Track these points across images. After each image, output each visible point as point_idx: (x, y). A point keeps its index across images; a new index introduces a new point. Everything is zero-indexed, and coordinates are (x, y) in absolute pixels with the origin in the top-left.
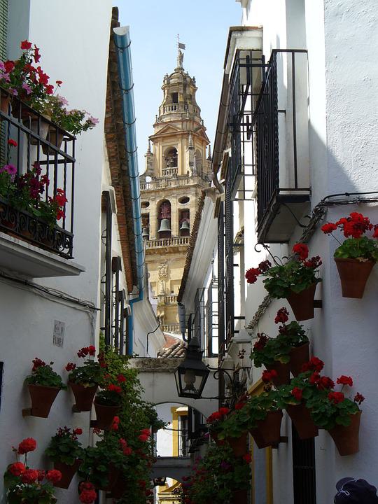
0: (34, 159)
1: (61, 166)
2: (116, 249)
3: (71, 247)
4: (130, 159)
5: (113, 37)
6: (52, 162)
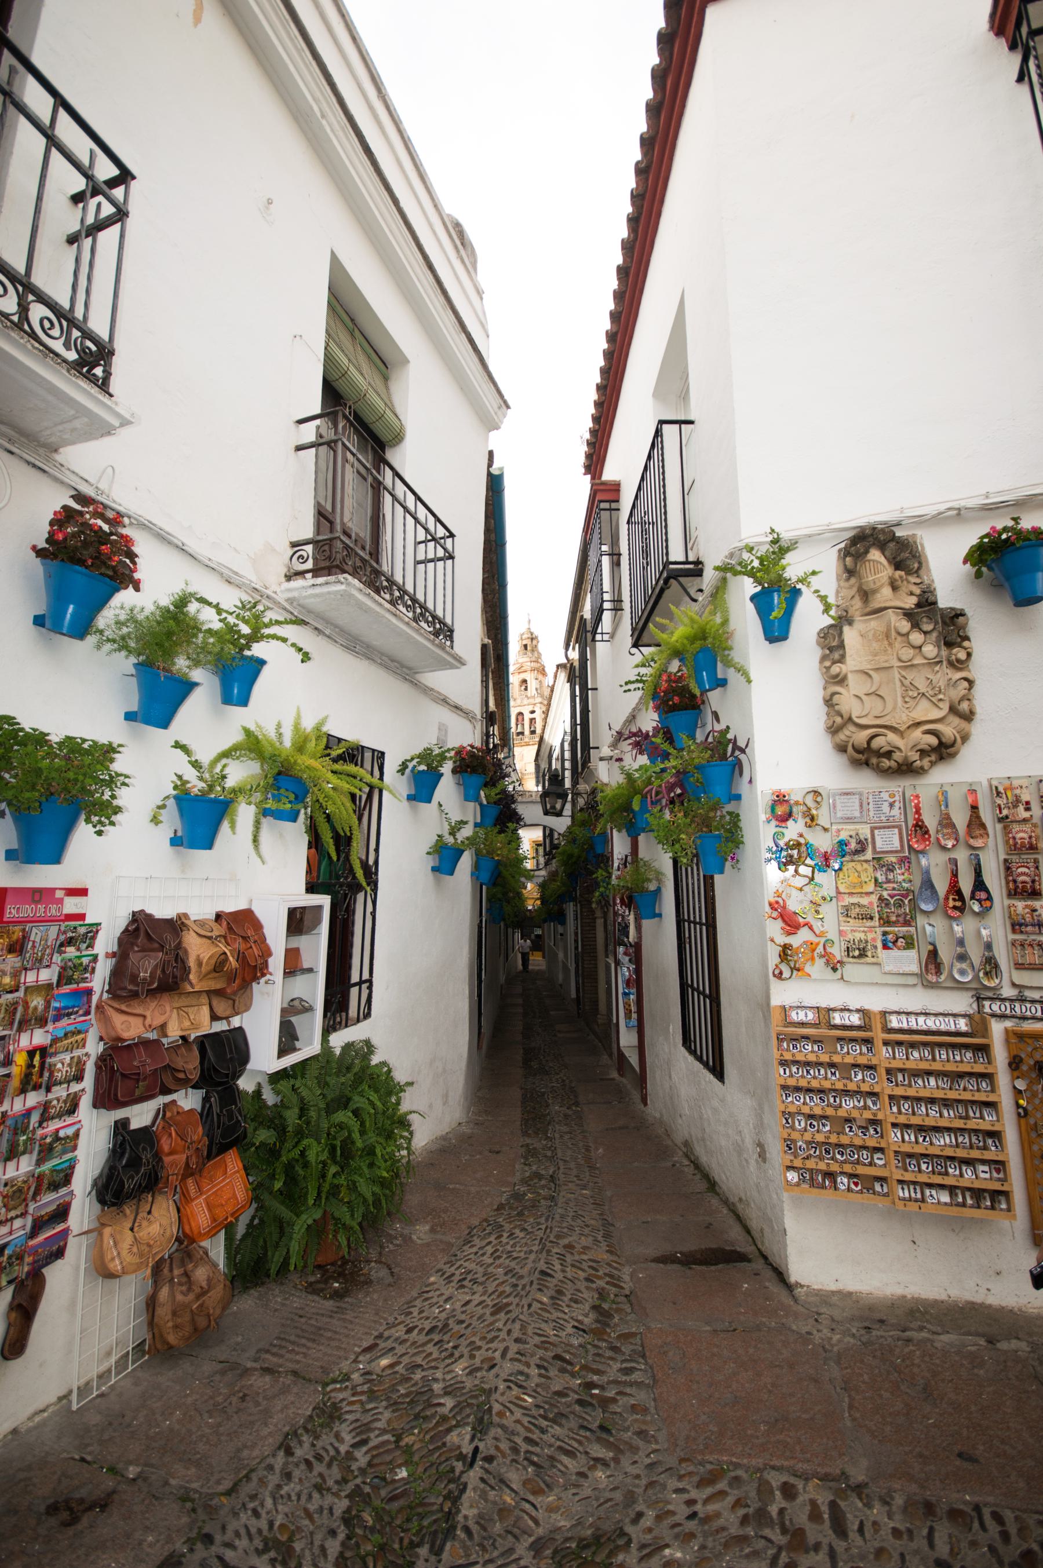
1: (440, 564)
5: (489, 474)
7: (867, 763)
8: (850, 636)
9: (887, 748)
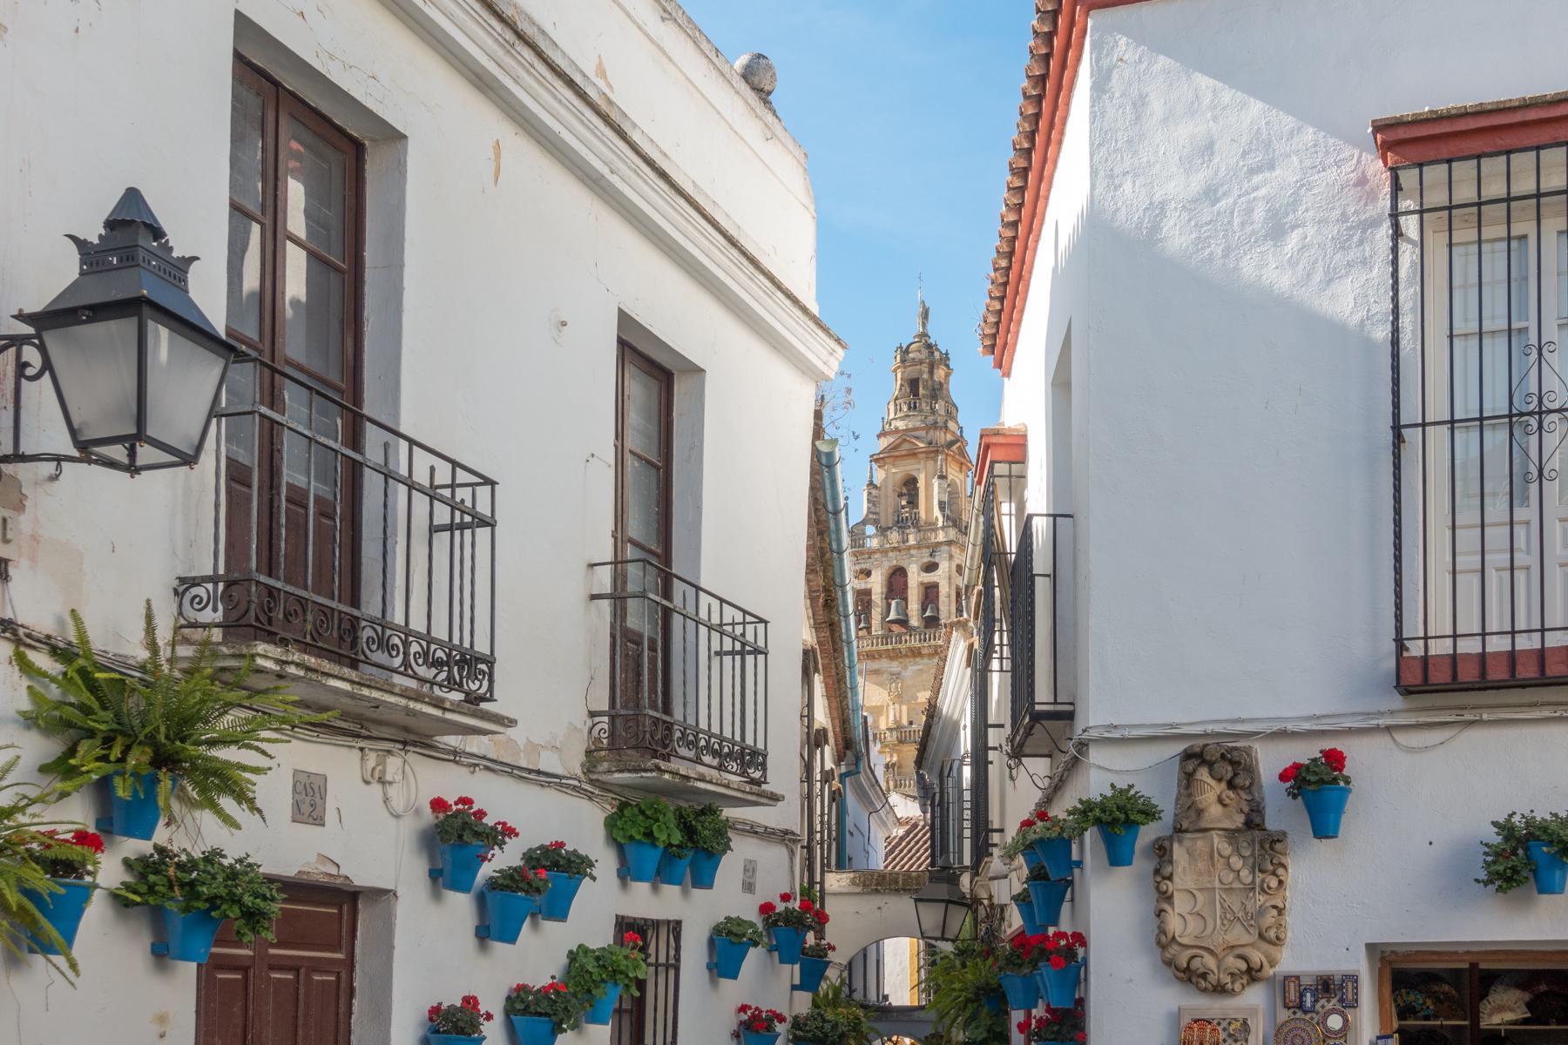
0: (715, 646)
2: (822, 717)
3: (765, 770)
4: (836, 563)
6: (738, 653)
7: (1190, 980)
8: (1178, 852)
9: (1202, 970)
